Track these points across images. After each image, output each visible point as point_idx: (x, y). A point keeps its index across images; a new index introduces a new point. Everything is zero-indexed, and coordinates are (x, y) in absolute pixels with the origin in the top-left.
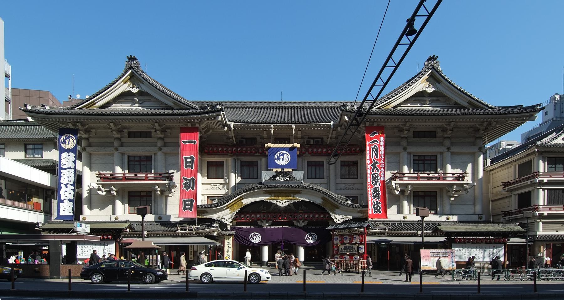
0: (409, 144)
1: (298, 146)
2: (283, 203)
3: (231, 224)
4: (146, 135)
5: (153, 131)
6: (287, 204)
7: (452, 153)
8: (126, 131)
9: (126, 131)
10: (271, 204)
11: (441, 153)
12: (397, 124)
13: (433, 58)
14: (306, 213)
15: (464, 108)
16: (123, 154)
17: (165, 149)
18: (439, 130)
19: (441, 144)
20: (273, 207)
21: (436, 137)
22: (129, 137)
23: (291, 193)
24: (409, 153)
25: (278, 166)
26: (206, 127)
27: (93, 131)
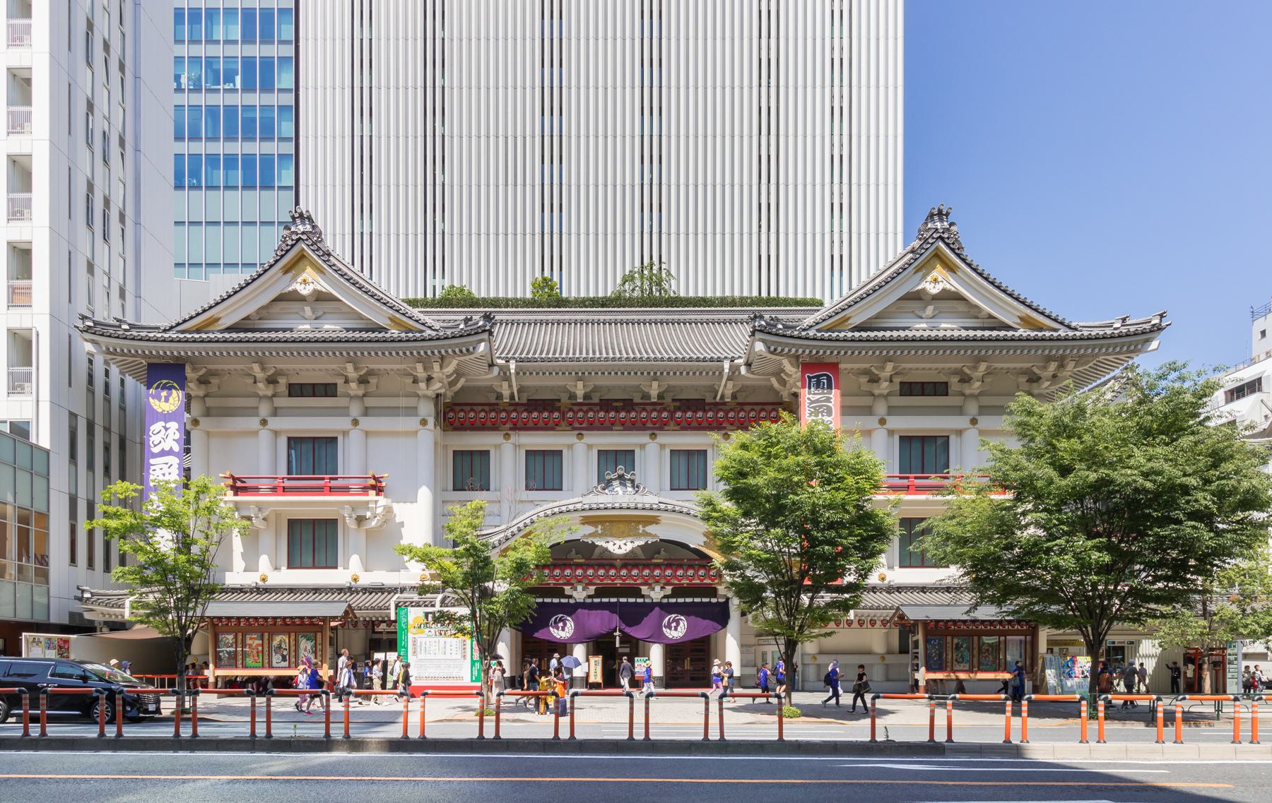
0: (892, 410)
2: (620, 546)
4: (328, 390)
5: (340, 381)
6: (629, 547)
7: (981, 433)
9: (283, 381)
10: (593, 546)
11: (959, 432)
13: (940, 213)
14: (669, 566)
15: (1008, 328)
16: (276, 433)
17: (366, 423)
18: (954, 380)
19: (959, 411)
20: (597, 551)
21: (947, 394)
22: (290, 395)
23: (639, 522)
24: (891, 433)
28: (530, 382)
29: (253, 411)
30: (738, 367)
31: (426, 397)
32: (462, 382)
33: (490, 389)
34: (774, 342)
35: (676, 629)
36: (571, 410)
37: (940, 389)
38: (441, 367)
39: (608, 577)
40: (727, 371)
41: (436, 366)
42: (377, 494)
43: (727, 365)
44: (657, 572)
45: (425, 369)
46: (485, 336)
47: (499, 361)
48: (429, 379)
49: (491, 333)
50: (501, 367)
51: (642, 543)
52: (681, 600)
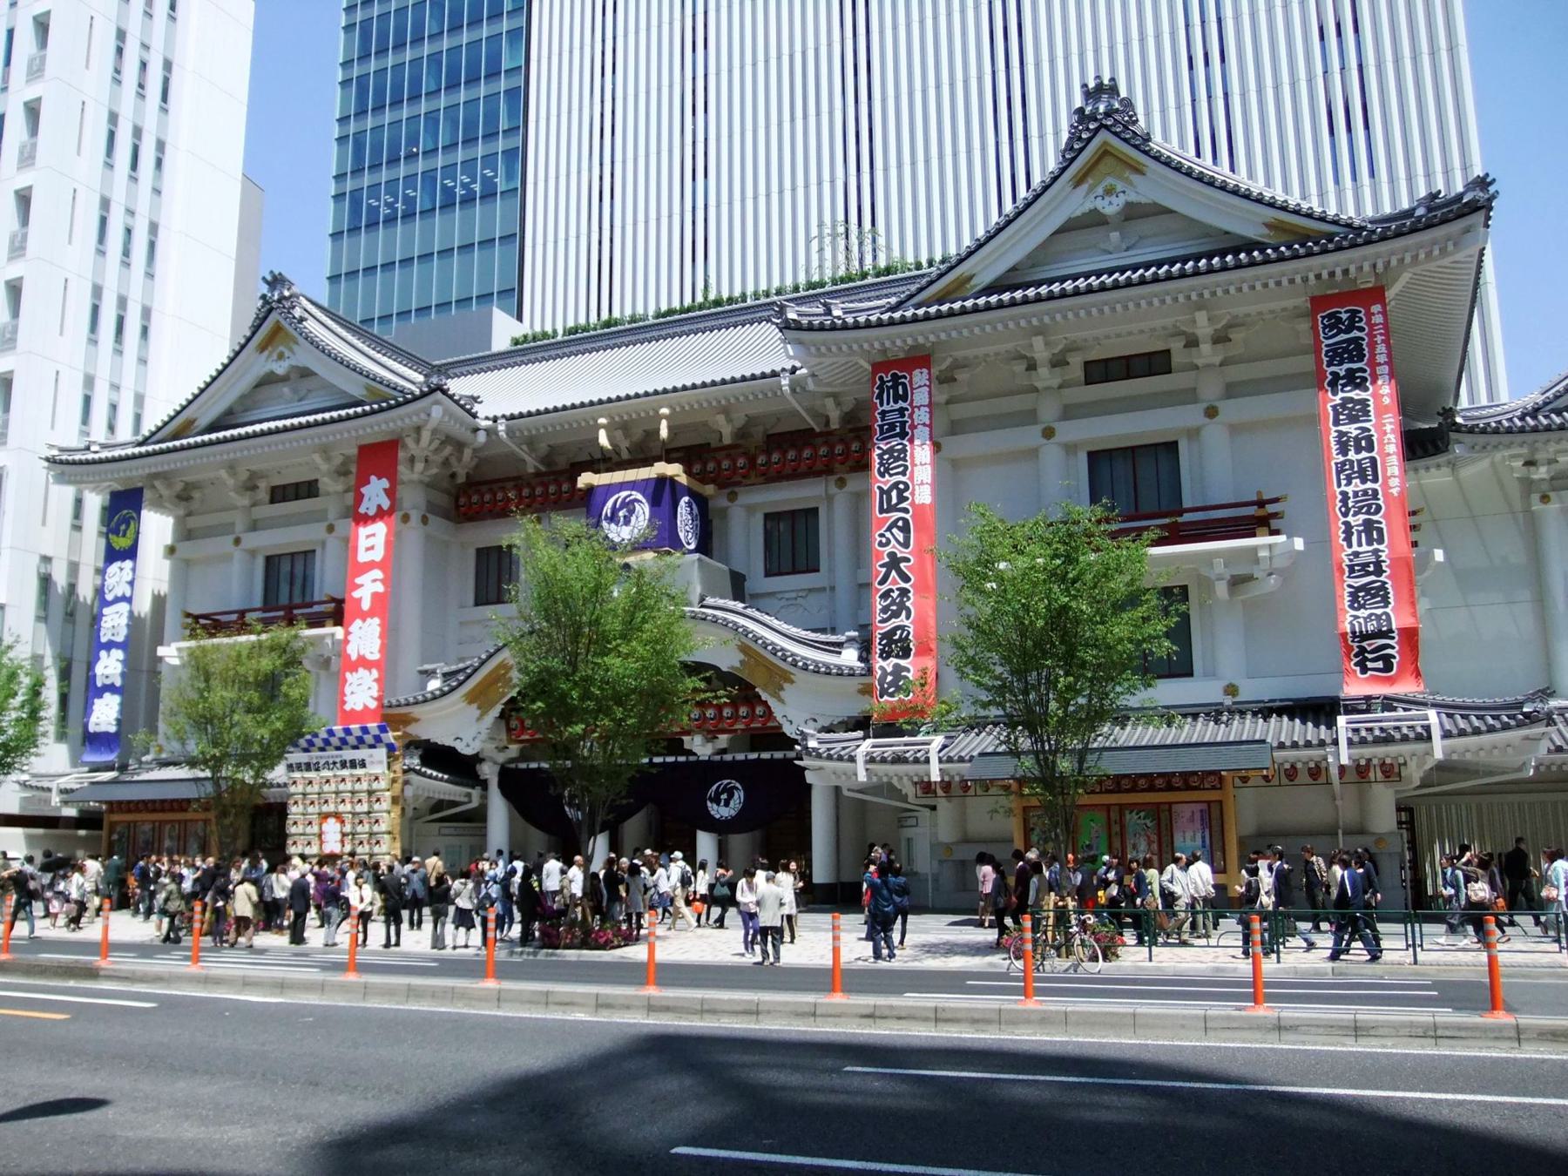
1: (674, 470)
4: (309, 489)
8: (263, 485)
9: (263, 485)
12: (1010, 346)
16: (253, 553)
22: (272, 501)
27: (196, 495)
29: (225, 529)
30: (805, 377)
31: (411, 482)
32: (467, 453)
35: (727, 804)
37: (1156, 363)
42: (336, 624)
50: (487, 430)
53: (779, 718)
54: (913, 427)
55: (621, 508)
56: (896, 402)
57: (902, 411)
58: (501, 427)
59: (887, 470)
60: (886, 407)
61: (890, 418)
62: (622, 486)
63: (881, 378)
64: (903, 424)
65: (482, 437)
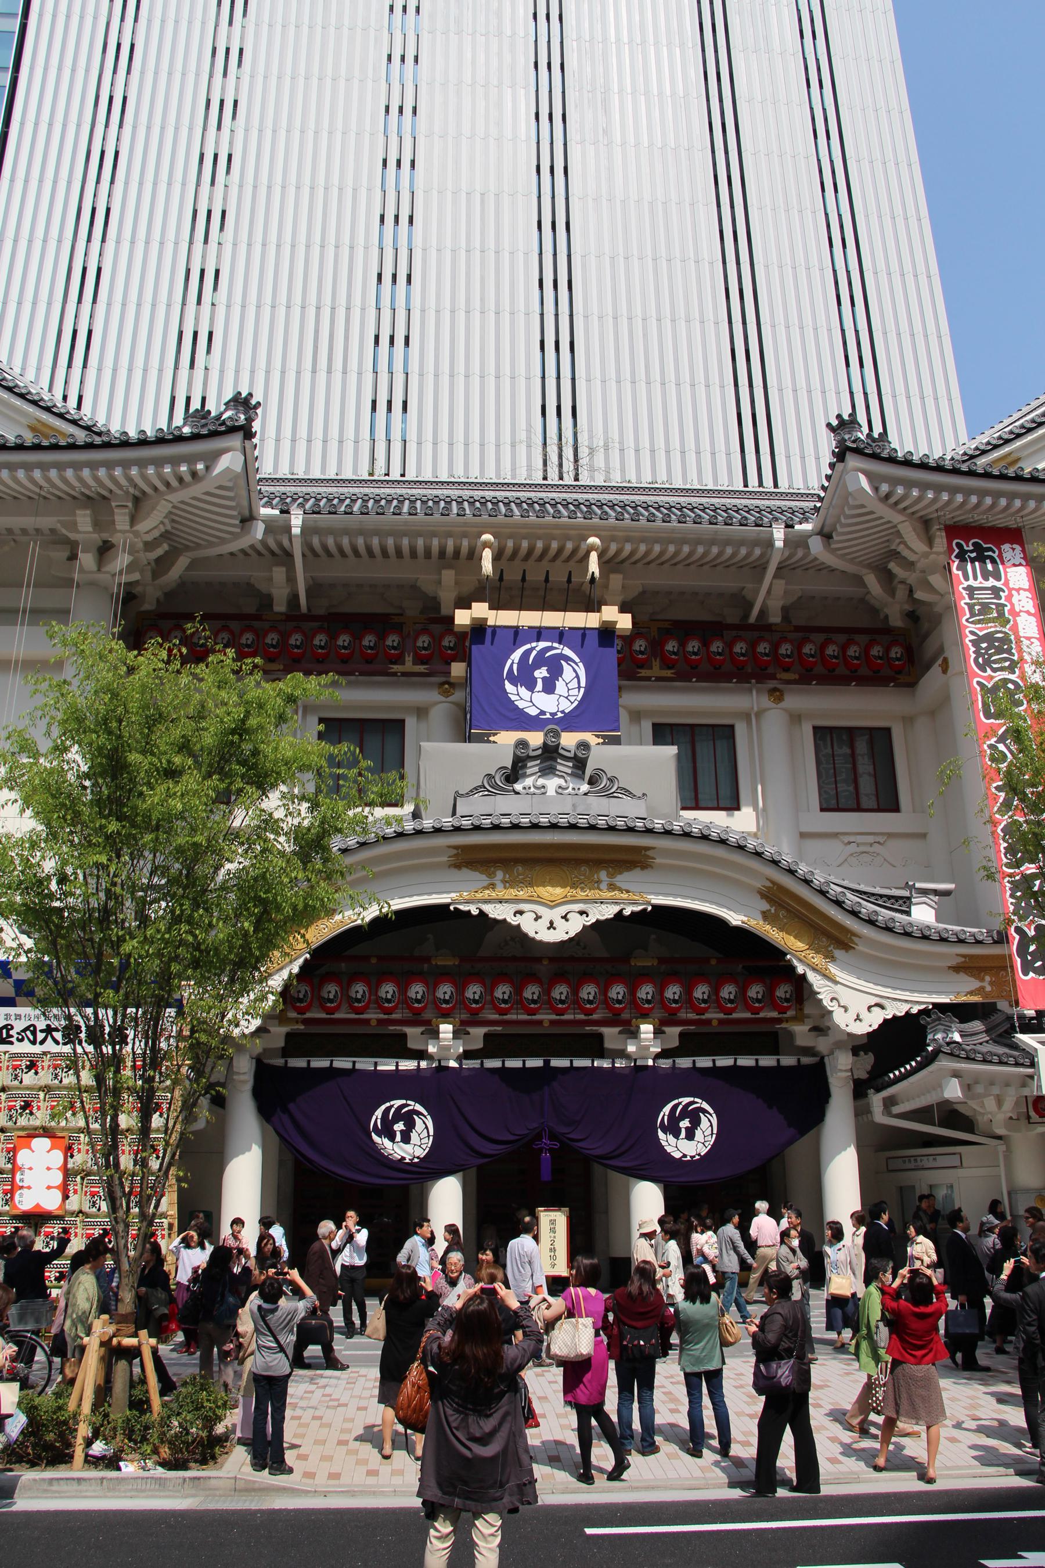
3: (259, 1044)
6: (574, 926)
25: (522, 721)
26: (166, 536)
28: (335, 572)
33: (249, 589)
34: (885, 479)
36: (425, 631)
38: (133, 520)
39: (518, 1001)
40: (779, 544)
41: (121, 520)
43: (779, 534)
44: (646, 991)
45: (97, 524)
46: (236, 441)
47: (265, 511)
48: (105, 550)
49: (249, 435)
50: (269, 523)
51: (608, 912)
52: (704, 1062)
53: (826, 1002)
54: (1015, 614)
55: (537, 665)
56: (986, 579)
57: (996, 591)
58: (296, 520)
59: (988, 663)
60: (971, 582)
61: (985, 597)
62: (539, 633)
63: (958, 545)
64: (1000, 607)
65: (259, 531)
